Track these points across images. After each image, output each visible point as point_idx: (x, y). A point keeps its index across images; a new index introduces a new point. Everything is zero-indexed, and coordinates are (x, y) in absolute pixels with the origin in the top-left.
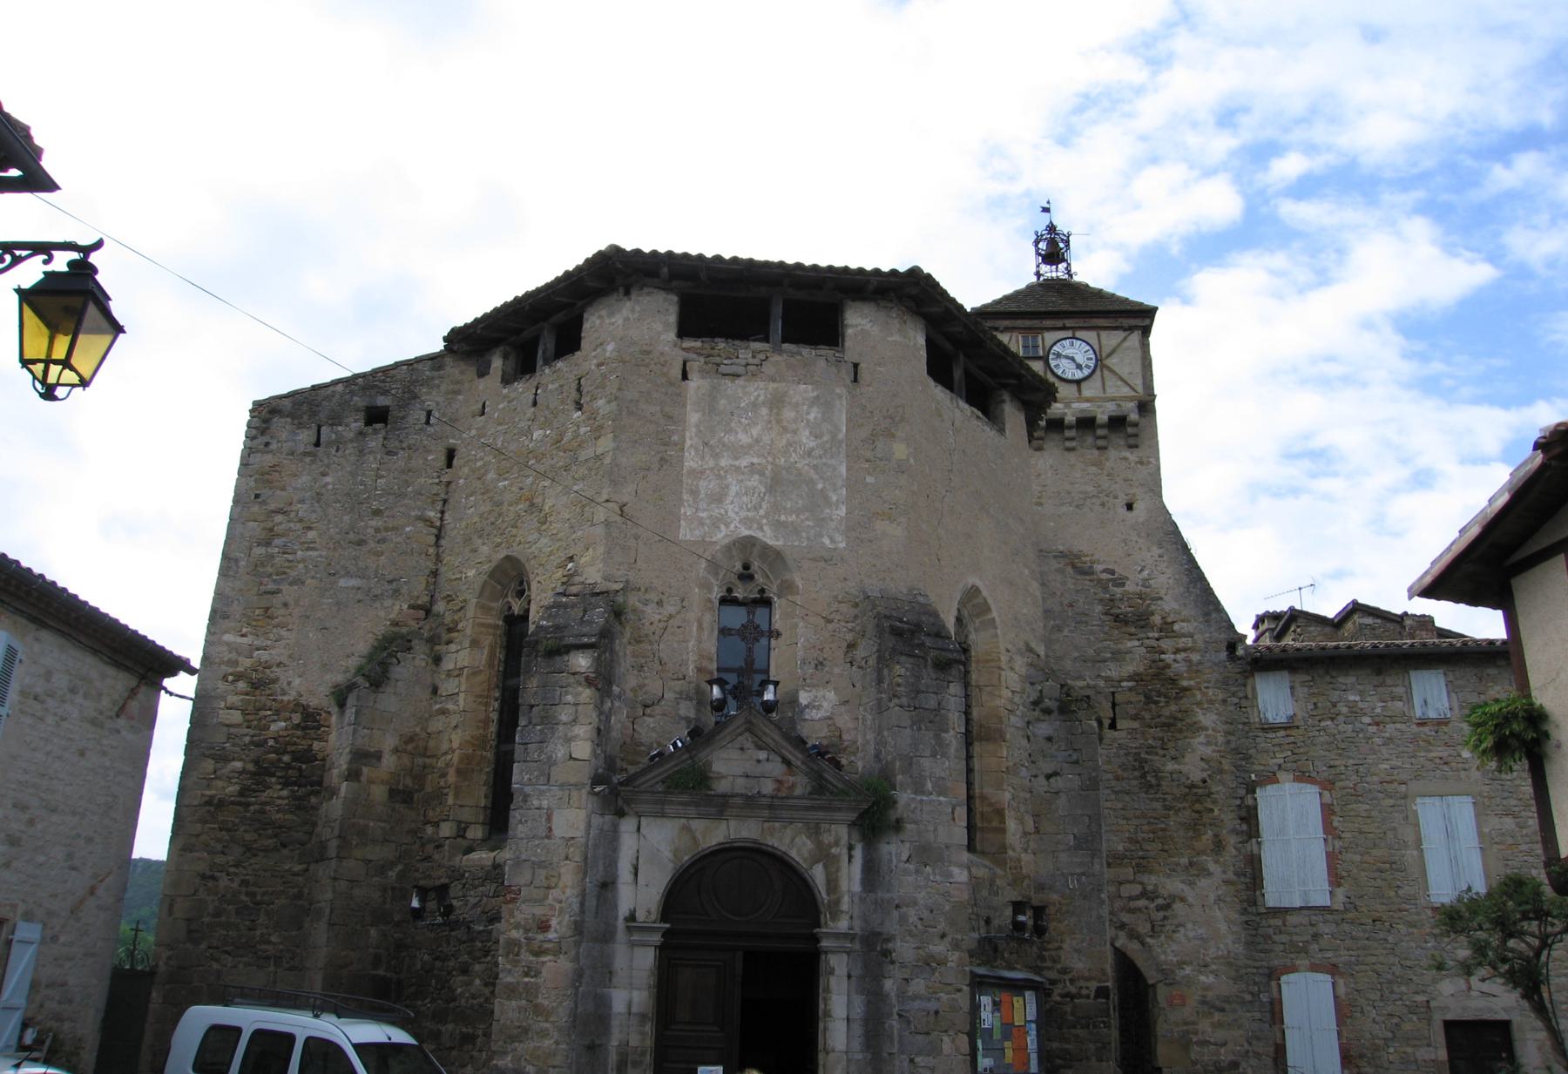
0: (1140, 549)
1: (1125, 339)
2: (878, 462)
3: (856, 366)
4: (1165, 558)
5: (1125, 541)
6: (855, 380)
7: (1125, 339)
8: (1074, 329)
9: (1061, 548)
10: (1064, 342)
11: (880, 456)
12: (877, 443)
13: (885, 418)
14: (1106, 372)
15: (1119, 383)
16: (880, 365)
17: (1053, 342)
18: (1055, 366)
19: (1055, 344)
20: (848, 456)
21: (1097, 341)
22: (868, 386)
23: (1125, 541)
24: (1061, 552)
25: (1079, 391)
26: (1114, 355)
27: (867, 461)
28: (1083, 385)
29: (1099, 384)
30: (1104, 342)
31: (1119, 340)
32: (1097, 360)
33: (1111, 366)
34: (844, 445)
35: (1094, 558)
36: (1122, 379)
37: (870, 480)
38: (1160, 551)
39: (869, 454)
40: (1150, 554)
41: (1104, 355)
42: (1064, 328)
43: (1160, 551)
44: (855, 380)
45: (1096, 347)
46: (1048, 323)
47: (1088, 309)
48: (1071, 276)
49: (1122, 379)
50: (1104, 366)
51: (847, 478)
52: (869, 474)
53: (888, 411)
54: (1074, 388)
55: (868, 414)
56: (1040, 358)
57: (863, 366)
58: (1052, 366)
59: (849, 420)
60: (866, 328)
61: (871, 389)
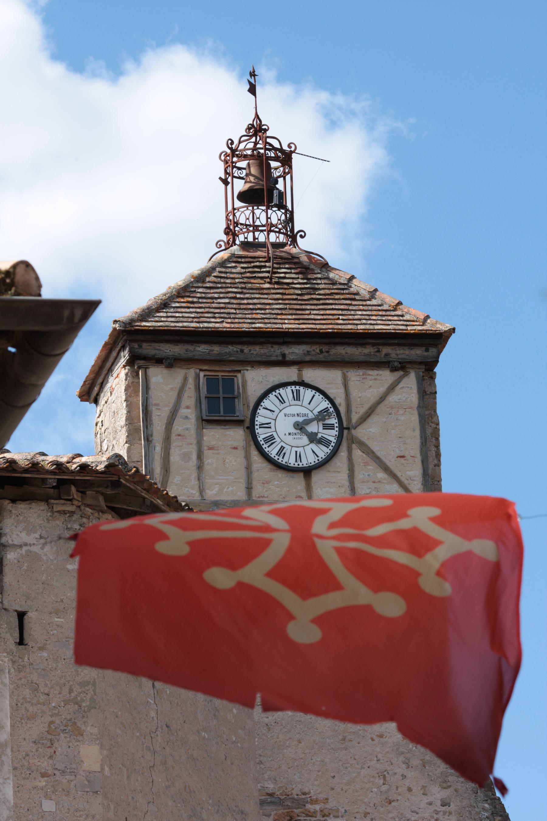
0: (410, 790)
1: (392, 388)
2: (58, 776)
3: (21, 615)
4: (453, 807)
5: (383, 775)
6: (21, 642)
7: (392, 388)
8: (300, 363)
9: (271, 786)
10: (282, 391)
11: (61, 766)
12: (56, 744)
13: (66, 702)
14: (357, 453)
15: (381, 475)
16: (57, 612)
17: (280, 474)
18: (266, 440)
19: (265, 395)
20: (15, 769)
21: (342, 390)
22: (42, 649)
23: (383, 775)
24: (271, 795)
25: (309, 488)
26: (373, 419)
27: (43, 775)
28: (317, 477)
29: (344, 476)
30: (354, 393)
31: (382, 390)
32: (342, 428)
33: (365, 439)
34: (9, 751)
35: (328, 806)
36: (386, 469)
37: (48, 806)
38: (445, 794)
39: (45, 765)
40: (425, 800)
41: (355, 418)
42: (283, 362)
43: (445, 794)
44: (21, 642)
45: (340, 401)
46: (256, 351)
47: (329, 328)
48: (293, 238)
49: (386, 469)
50: (353, 440)
51: (16, 805)
52: (47, 797)
53: (71, 691)
54: (298, 481)
55: (42, 698)
56: (239, 423)
57: (31, 617)
58: (260, 438)
59: (15, 708)
60: (34, 549)
61: (45, 654)
